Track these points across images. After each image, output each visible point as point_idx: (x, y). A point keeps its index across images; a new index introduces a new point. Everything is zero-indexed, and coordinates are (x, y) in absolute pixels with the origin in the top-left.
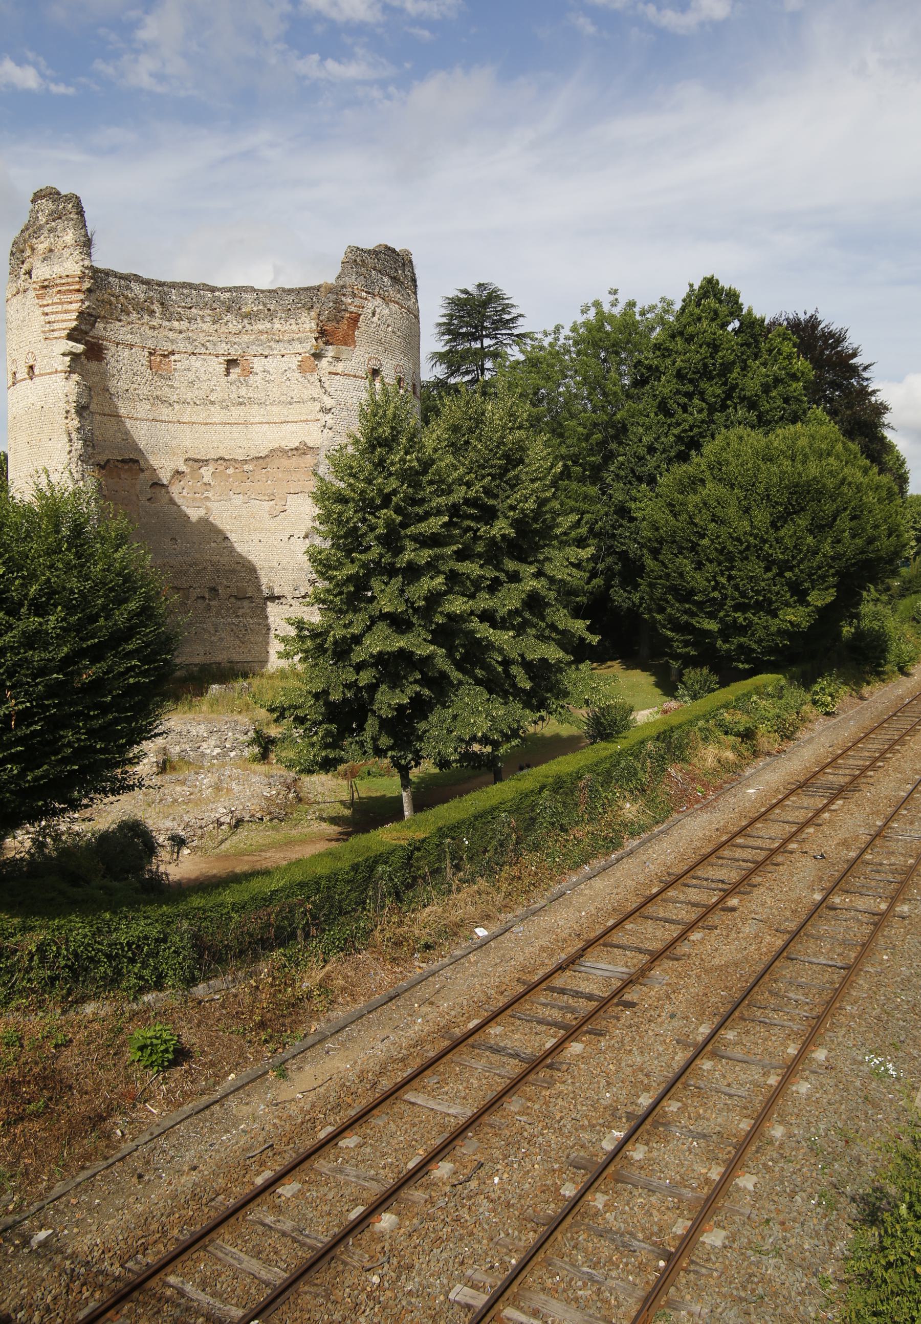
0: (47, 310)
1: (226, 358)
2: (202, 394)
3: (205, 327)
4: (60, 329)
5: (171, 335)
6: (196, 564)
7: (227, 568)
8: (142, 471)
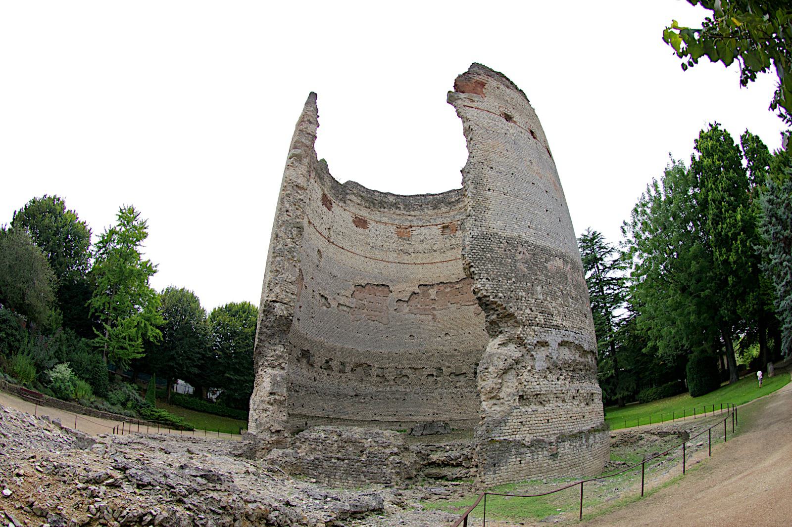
1: (442, 225)
2: (428, 247)
3: (429, 212)
5: (410, 218)
6: (427, 352)
7: (448, 354)
8: (391, 292)
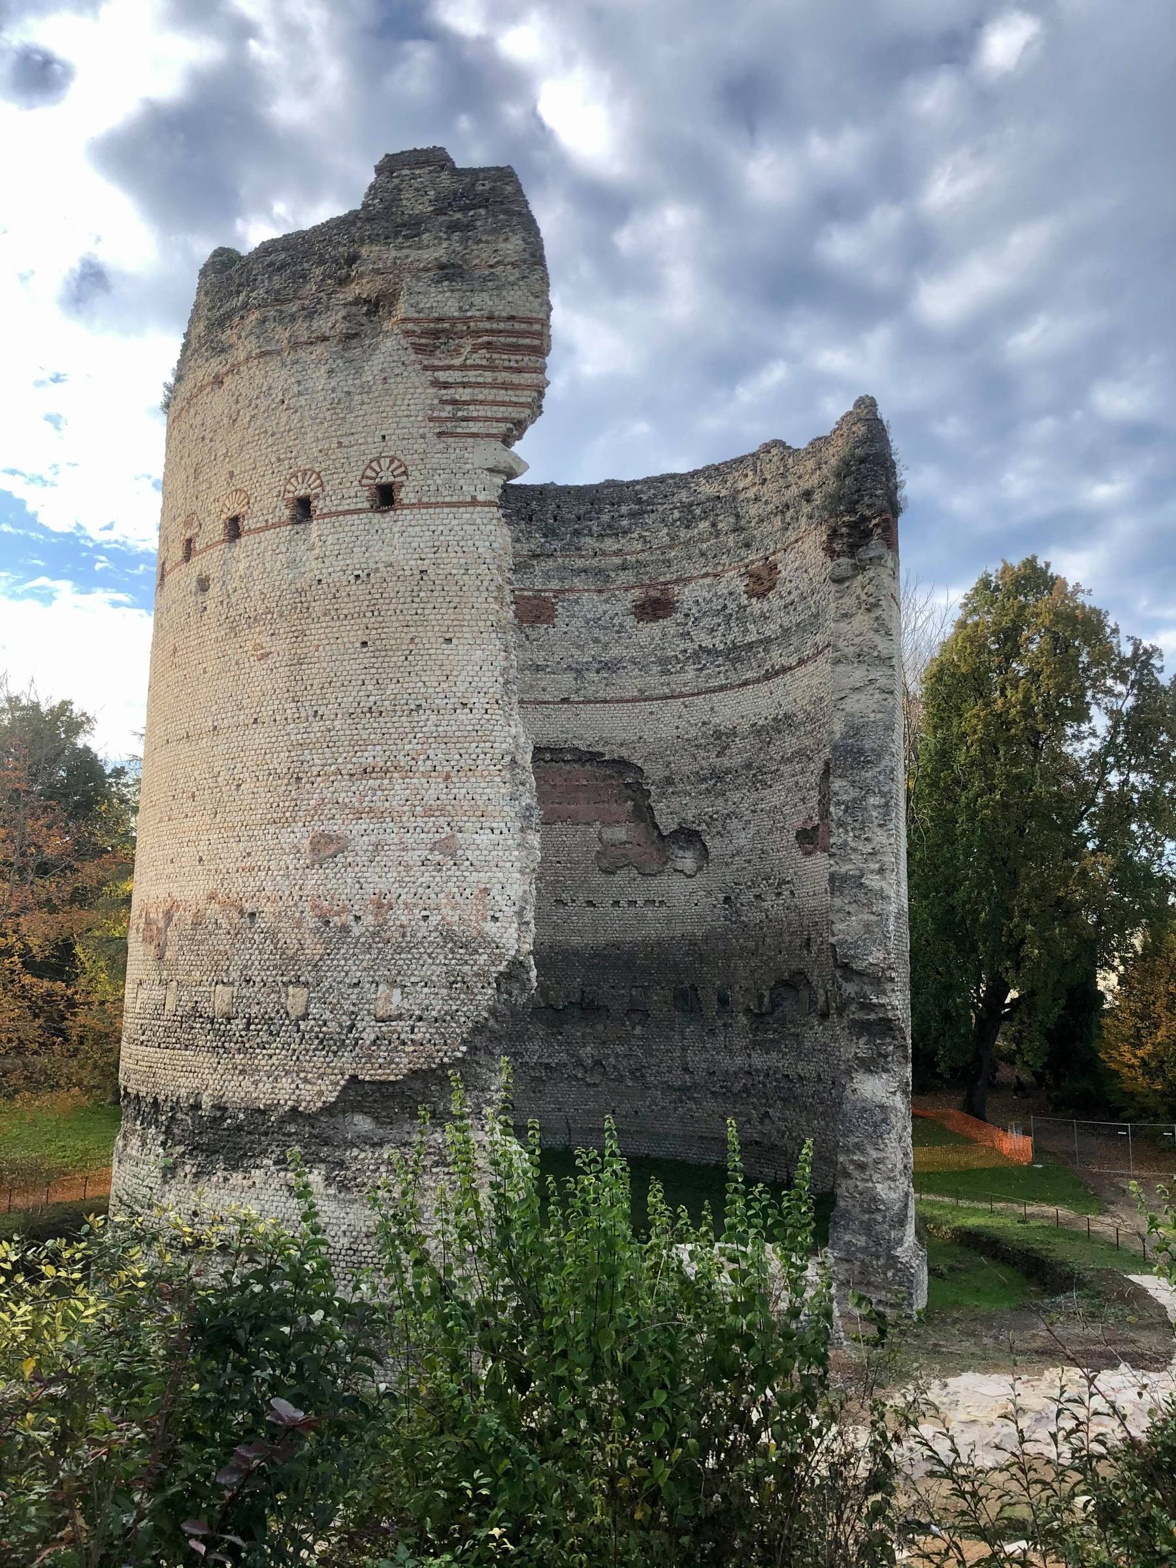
0: (442, 376)
4: (487, 419)
